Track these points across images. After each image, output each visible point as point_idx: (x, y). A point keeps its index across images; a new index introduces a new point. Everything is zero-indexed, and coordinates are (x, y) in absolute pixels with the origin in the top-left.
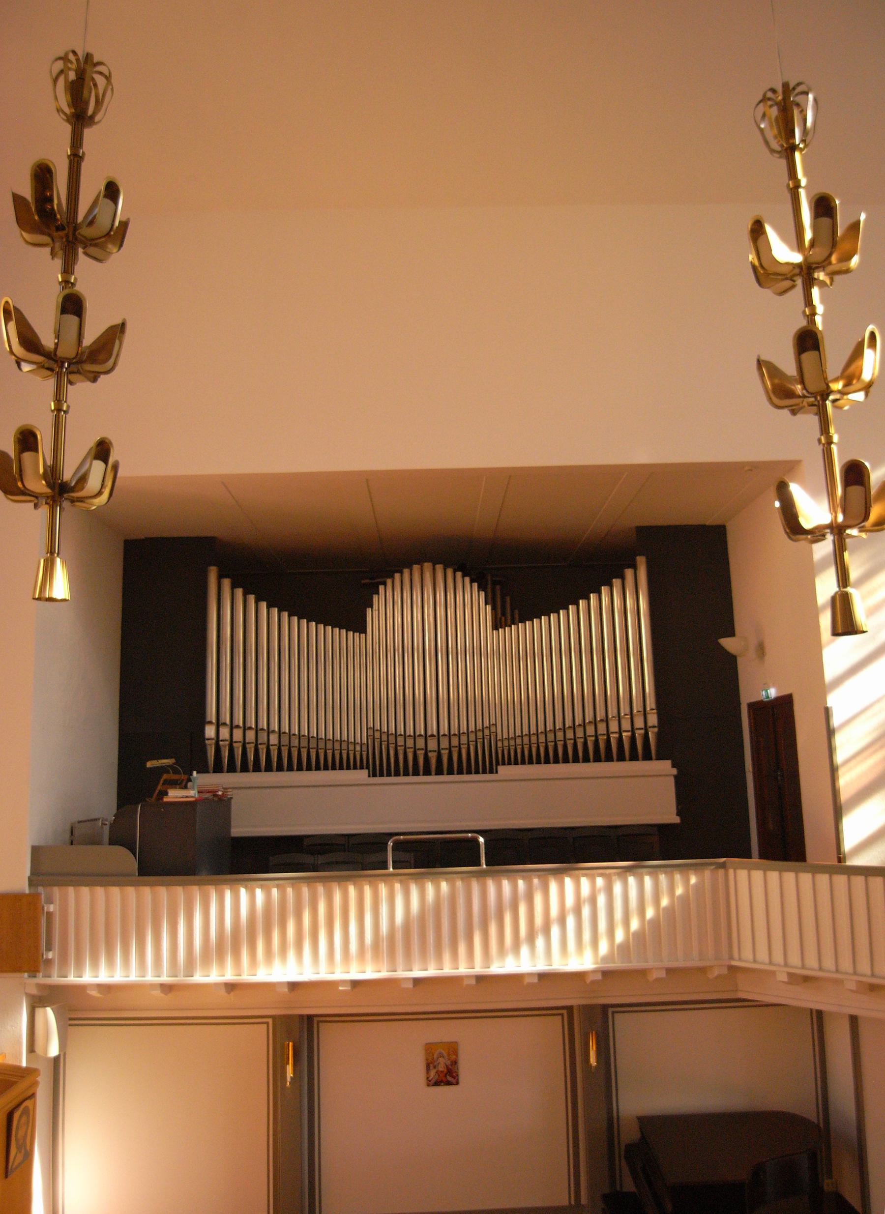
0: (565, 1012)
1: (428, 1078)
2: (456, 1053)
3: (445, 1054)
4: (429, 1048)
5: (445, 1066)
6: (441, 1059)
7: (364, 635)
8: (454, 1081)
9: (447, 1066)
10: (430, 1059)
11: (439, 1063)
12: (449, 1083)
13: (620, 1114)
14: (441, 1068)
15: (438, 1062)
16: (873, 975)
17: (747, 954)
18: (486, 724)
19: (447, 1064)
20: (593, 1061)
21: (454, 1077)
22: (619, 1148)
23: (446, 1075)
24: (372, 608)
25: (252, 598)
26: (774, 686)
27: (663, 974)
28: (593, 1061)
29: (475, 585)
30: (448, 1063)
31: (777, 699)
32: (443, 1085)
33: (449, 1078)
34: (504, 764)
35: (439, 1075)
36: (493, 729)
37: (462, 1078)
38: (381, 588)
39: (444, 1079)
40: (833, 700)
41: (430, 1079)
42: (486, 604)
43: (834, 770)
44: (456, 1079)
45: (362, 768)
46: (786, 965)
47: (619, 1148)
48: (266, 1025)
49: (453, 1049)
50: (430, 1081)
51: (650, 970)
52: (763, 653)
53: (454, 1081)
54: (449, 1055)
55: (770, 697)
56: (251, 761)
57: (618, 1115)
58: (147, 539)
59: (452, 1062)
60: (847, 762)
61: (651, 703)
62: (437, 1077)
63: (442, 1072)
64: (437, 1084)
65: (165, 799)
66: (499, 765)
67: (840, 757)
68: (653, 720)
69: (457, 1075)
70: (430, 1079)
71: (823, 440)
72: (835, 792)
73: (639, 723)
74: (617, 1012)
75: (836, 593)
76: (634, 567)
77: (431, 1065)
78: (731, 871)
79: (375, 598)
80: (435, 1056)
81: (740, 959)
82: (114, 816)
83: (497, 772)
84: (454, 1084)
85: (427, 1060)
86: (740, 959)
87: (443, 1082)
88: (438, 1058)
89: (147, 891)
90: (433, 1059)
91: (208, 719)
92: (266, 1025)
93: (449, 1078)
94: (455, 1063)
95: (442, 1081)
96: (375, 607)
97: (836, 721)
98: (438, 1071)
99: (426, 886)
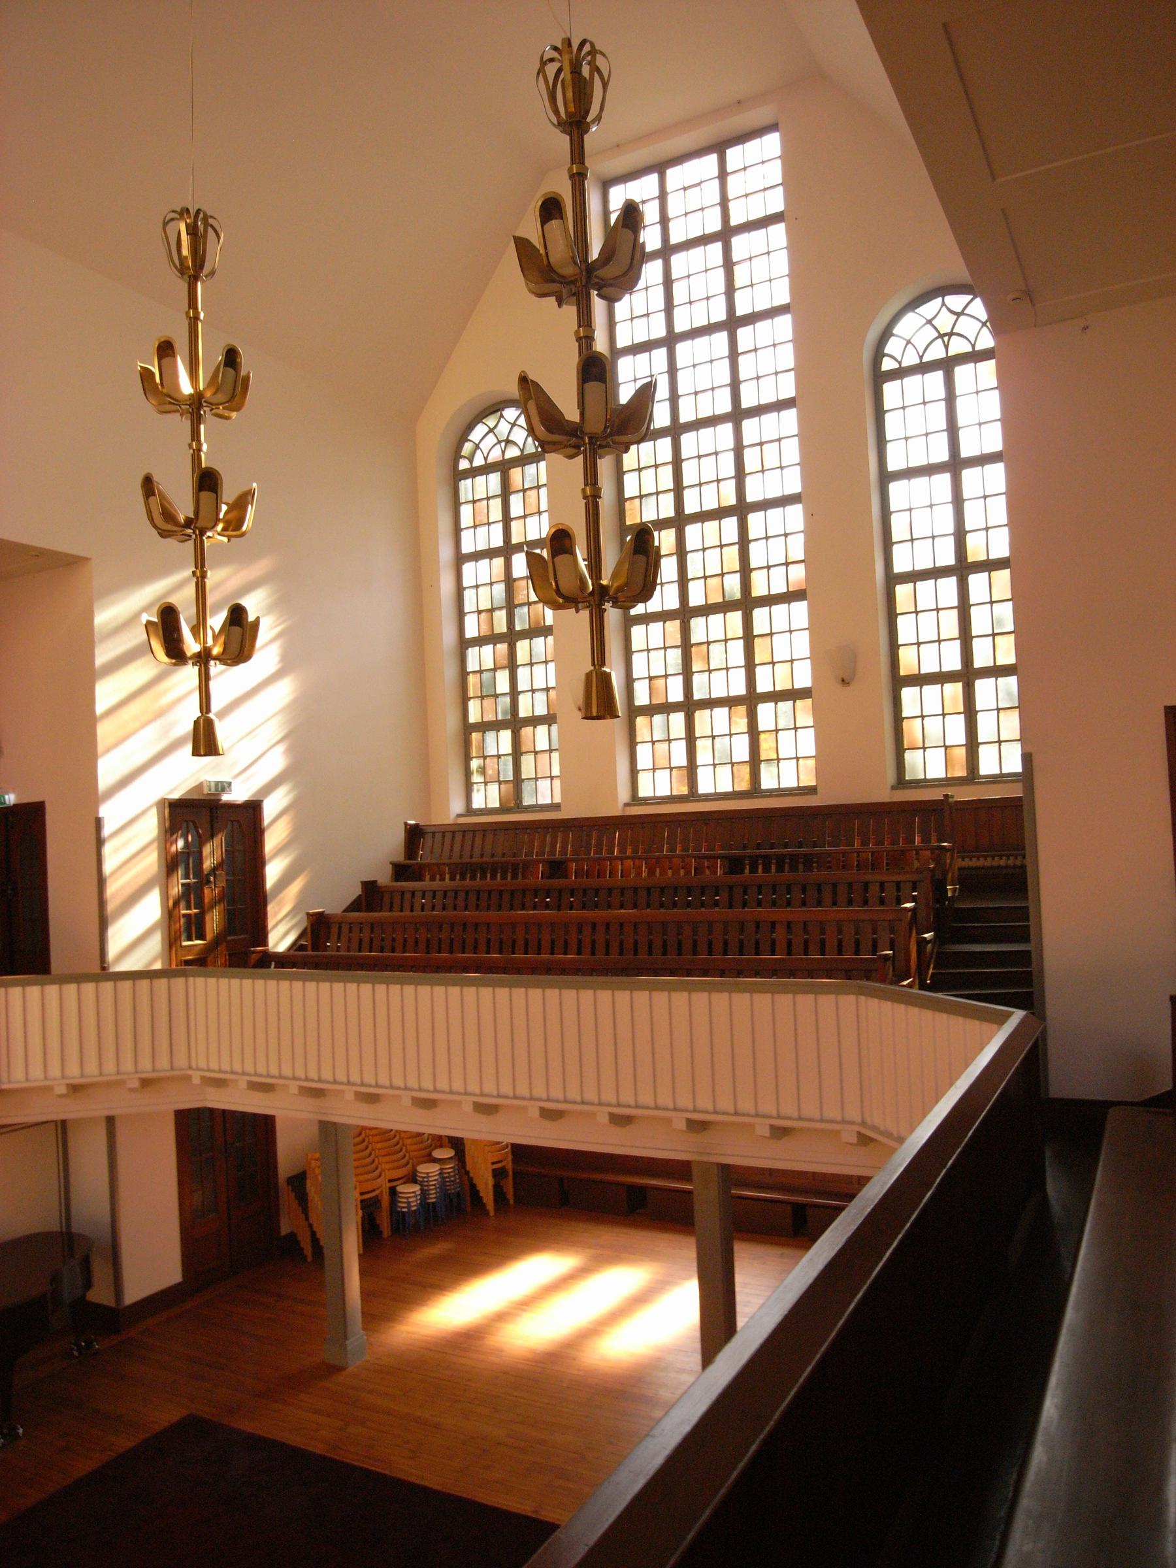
16: (154, 1071)
17: (18, 1074)
31: (17, 808)
40: (104, 811)
43: (101, 882)
46: (63, 1077)
55: (7, 802)
60: (114, 873)
67: (108, 868)
71: (198, 574)
72: (102, 903)
75: (198, 718)
81: (10, 1082)
86: (10, 1082)
97: (106, 831)
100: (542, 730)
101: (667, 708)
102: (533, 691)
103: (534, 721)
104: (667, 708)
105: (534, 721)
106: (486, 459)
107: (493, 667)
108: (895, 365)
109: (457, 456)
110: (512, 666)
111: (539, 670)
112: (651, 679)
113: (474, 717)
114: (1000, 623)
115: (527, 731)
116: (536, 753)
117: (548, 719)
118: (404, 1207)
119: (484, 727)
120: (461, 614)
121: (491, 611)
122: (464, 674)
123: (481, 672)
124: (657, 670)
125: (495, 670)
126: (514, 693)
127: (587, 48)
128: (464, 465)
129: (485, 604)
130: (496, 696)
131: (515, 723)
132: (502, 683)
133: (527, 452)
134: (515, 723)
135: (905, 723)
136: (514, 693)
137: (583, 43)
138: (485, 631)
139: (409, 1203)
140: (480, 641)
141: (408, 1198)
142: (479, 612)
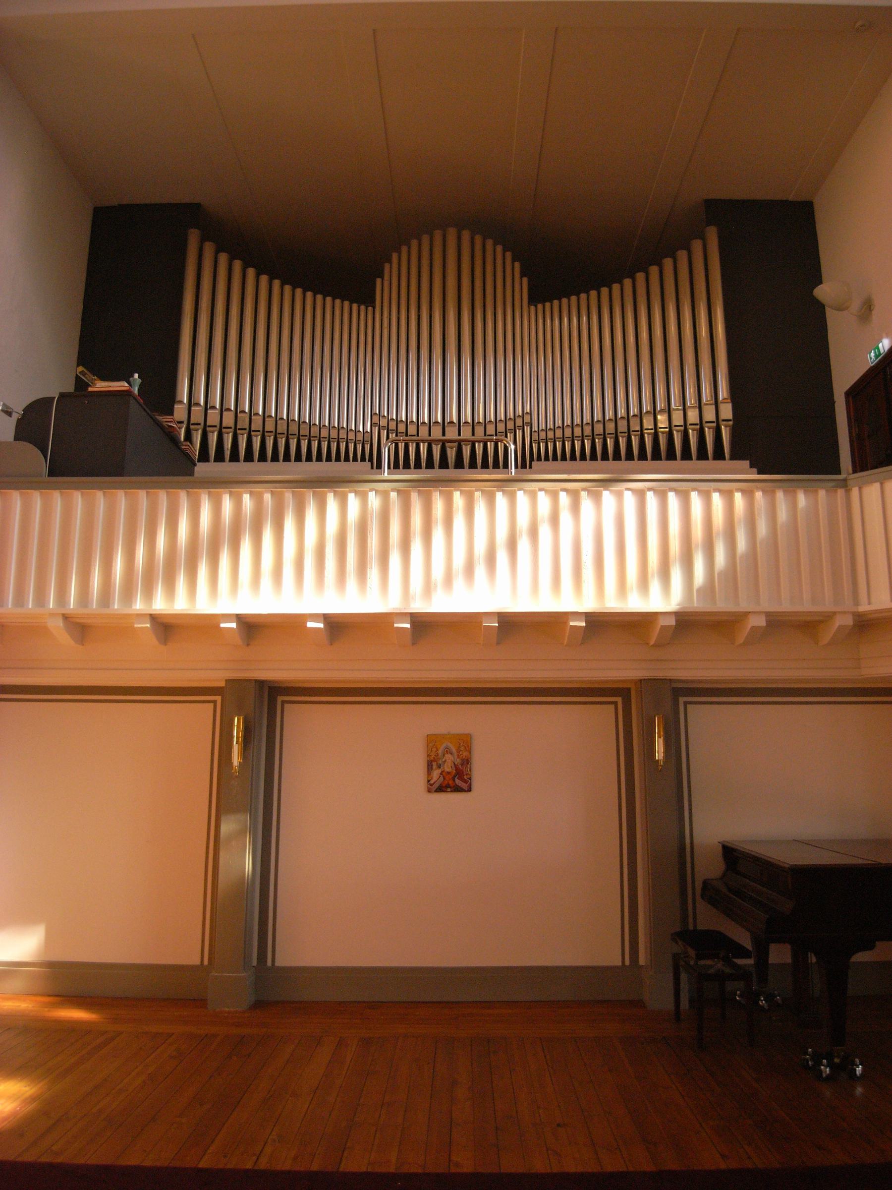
0: (619, 700)
1: (429, 781)
2: (469, 749)
3: (454, 750)
4: (432, 741)
5: (453, 766)
6: (448, 756)
7: (370, 309)
8: (465, 786)
9: (455, 765)
10: (433, 754)
11: (445, 761)
12: (457, 789)
13: (695, 841)
14: (448, 768)
15: (444, 760)
18: (519, 412)
19: (456, 763)
20: (659, 754)
21: (466, 782)
22: (694, 888)
23: (455, 776)
24: (383, 279)
25: (237, 265)
26: (887, 337)
27: (761, 622)
28: (659, 754)
29: (509, 255)
30: (458, 761)
32: (451, 791)
33: (458, 782)
34: (539, 459)
35: (444, 779)
36: (527, 419)
37: (475, 785)
38: (395, 256)
39: (450, 782)
41: (432, 782)
42: (521, 277)
44: (468, 783)
45: (363, 459)
47: (693, 882)
48: (212, 705)
49: (465, 743)
50: (431, 785)
51: (746, 614)
52: (870, 309)
53: (465, 786)
54: (459, 750)
55: (882, 351)
56: (228, 449)
57: (692, 843)
58: (122, 207)
59: (463, 760)
61: (723, 392)
62: (442, 778)
63: (448, 773)
64: (441, 789)
65: (90, 389)
66: (534, 461)
68: (727, 411)
69: (470, 779)
70: (432, 782)
73: (709, 415)
74: (691, 703)
76: (703, 238)
77: (434, 764)
78: (855, 492)
79: (387, 266)
80: (440, 752)
82: (23, 411)
83: (530, 467)
84: (465, 791)
85: (428, 756)
87: (451, 787)
88: (444, 755)
89: (57, 497)
90: (438, 755)
91: (178, 398)
92: (212, 705)
93: (458, 782)
94: (467, 761)
95: (448, 786)
96: (386, 277)
98: (442, 772)
99: (433, 498)
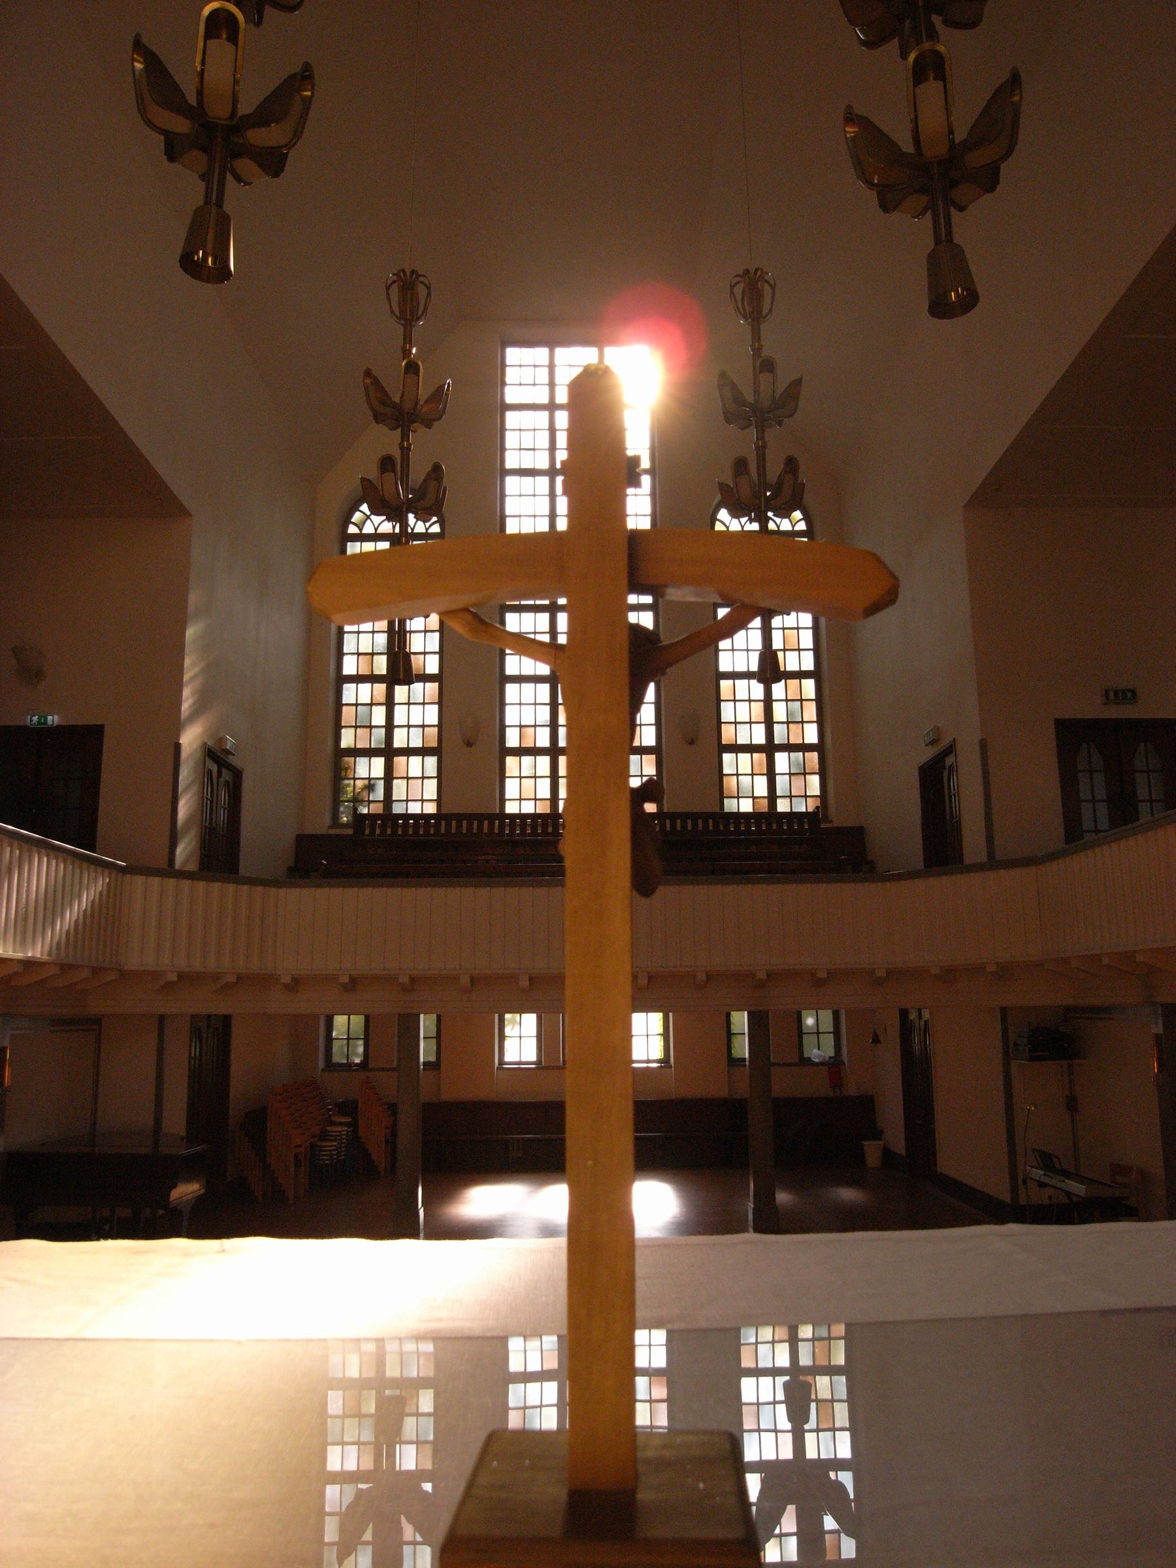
100: (415, 761)
101: (535, 751)
102: (409, 726)
103: (408, 752)
104: (535, 751)
105: (408, 752)
106: (376, 529)
107: (370, 702)
108: (724, 528)
109: (347, 521)
110: (390, 704)
111: (416, 710)
112: (521, 726)
113: (344, 744)
114: (793, 714)
115: (400, 761)
116: (408, 778)
117: (422, 752)
118: (327, 1160)
119: (356, 752)
120: (340, 654)
121: (373, 654)
122: (339, 705)
123: (357, 705)
124: (528, 720)
125: (371, 704)
126: (390, 726)
127: (759, 273)
128: (352, 529)
129: (365, 647)
130: (371, 727)
131: (389, 752)
132: (379, 716)
133: (416, 531)
134: (389, 752)
135: (725, 779)
136: (390, 726)
137: (756, 270)
138: (364, 671)
139: (331, 1156)
140: (358, 679)
141: (330, 1151)
142: (359, 654)
